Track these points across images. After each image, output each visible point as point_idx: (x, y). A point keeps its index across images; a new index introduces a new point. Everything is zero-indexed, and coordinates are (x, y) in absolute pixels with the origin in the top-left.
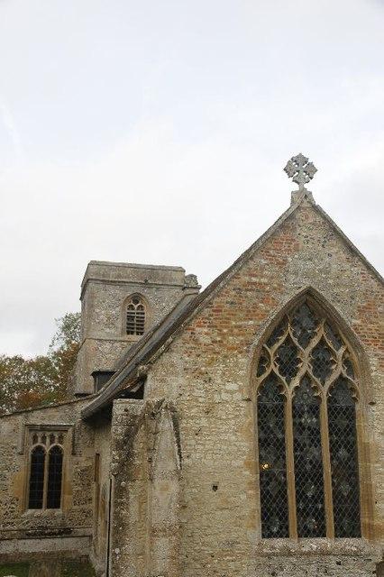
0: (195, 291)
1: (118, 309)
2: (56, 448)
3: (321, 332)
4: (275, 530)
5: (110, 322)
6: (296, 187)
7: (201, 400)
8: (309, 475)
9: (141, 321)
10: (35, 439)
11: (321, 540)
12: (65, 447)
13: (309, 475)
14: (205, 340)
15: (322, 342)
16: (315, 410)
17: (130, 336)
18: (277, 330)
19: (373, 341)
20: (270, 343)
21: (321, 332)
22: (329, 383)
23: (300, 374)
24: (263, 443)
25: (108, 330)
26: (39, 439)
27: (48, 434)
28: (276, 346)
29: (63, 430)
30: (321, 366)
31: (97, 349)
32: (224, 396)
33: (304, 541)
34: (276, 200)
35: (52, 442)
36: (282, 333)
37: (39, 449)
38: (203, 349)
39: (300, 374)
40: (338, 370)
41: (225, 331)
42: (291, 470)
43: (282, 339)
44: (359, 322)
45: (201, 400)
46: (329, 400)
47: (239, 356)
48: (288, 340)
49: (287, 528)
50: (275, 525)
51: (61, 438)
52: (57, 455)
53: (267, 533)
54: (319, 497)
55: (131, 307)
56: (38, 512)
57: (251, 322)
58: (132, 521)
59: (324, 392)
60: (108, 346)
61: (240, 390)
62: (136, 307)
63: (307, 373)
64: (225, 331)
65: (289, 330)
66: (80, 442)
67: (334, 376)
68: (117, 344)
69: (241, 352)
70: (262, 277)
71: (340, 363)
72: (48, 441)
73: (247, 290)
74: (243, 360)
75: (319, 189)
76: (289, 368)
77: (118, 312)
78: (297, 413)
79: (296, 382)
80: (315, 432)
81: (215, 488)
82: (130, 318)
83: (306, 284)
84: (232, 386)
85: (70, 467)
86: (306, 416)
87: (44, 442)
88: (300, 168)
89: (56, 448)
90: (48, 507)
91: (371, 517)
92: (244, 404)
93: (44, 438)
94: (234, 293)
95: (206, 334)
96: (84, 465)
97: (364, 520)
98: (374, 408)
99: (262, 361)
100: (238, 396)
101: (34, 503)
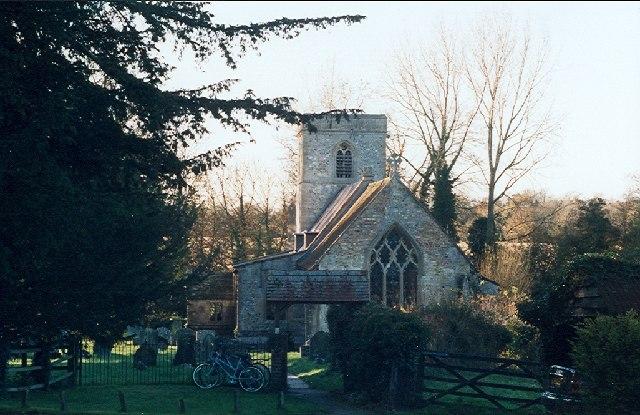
1: (328, 156)
5: (322, 168)
16: (397, 279)
18: (380, 243)
20: (377, 248)
21: (402, 242)
22: (405, 264)
25: (320, 174)
30: (401, 257)
31: (311, 191)
48: (385, 246)
55: (340, 152)
59: (402, 270)
76: (385, 260)
78: (389, 279)
79: (388, 266)
82: (339, 161)
99: (373, 256)
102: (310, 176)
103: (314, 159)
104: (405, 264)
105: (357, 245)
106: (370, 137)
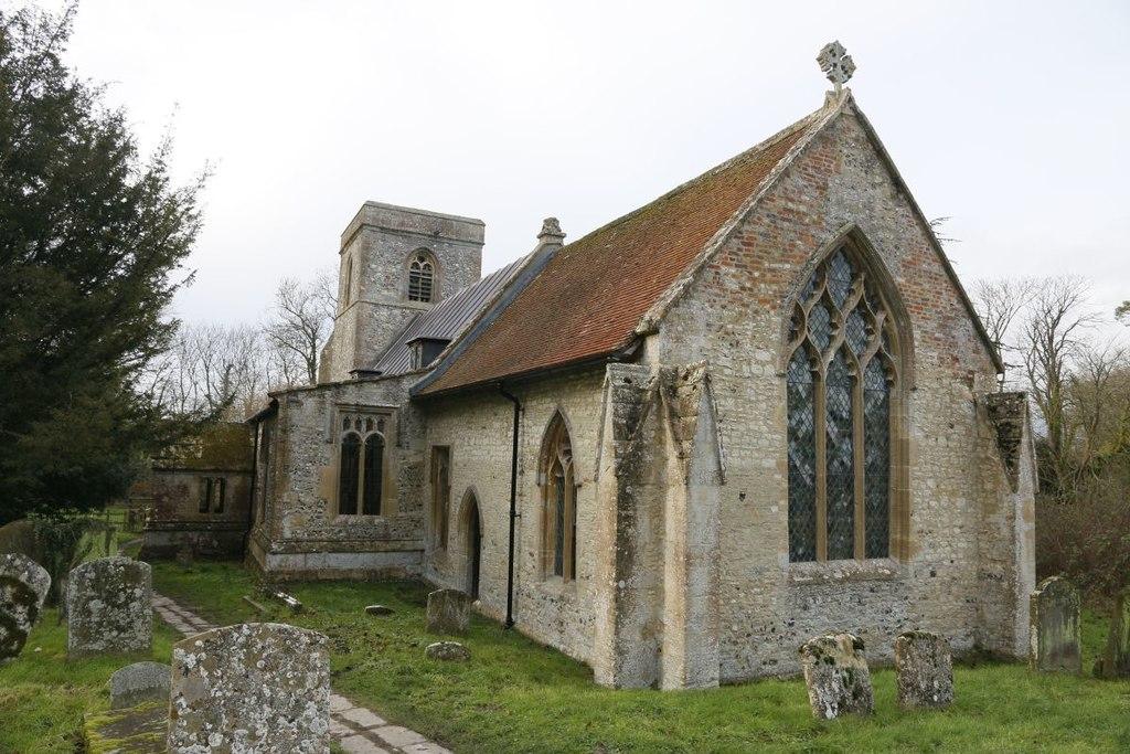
0: (557, 240)
1: (399, 267)
2: (375, 437)
4: (801, 551)
6: (831, 87)
7: (727, 371)
8: (842, 482)
9: (427, 283)
10: (346, 424)
11: (853, 562)
12: (387, 436)
13: (842, 482)
14: (732, 285)
17: (413, 302)
19: (916, 308)
20: (808, 296)
24: (792, 434)
25: (386, 292)
26: (353, 424)
27: (365, 417)
29: (384, 413)
31: (371, 316)
32: (756, 369)
33: (834, 564)
34: (806, 98)
35: (369, 428)
37: (352, 438)
38: (729, 297)
39: (837, 344)
41: (756, 274)
42: (822, 475)
43: (819, 294)
45: (727, 371)
47: (772, 312)
49: (814, 548)
50: (801, 545)
51: (381, 424)
52: (375, 445)
53: (795, 557)
54: (850, 510)
56: (352, 519)
57: (787, 266)
58: (640, 542)
60: (384, 313)
61: (773, 362)
62: (421, 265)
63: (844, 344)
64: (756, 274)
66: (408, 429)
68: (396, 312)
69: (774, 308)
71: (879, 333)
72: (364, 426)
73: (784, 220)
74: (776, 319)
75: (866, 93)
77: (400, 271)
81: (742, 496)
82: (414, 279)
83: (850, 219)
84: (764, 356)
85: (394, 464)
87: (358, 428)
88: (836, 62)
89: (375, 436)
90: (364, 513)
91: (905, 529)
92: (776, 381)
93: (358, 423)
94: (766, 221)
95: (734, 276)
96: (412, 460)
97: (895, 536)
98: (915, 395)
100: (770, 370)
101: (347, 506)
102: (373, 297)
103: (379, 271)
105: (763, 279)
106: (462, 252)
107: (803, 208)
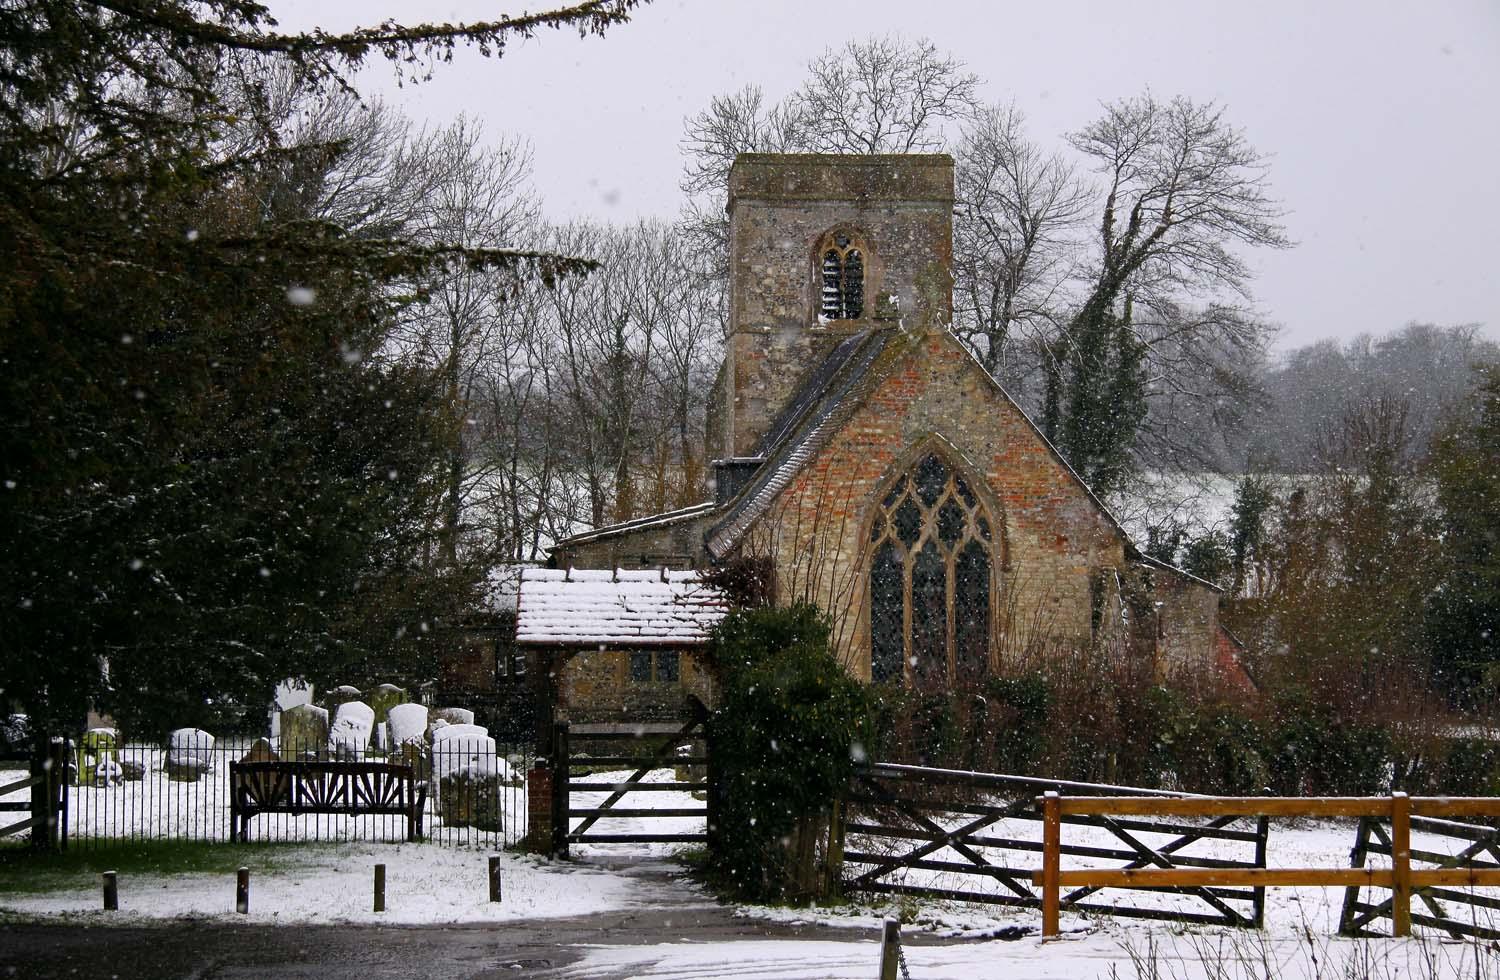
3: (950, 488)
15: (951, 500)
20: (888, 501)
21: (950, 488)
22: (958, 546)
23: (923, 538)
28: (895, 506)
30: (950, 527)
36: (901, 491)
40: (971, 531)
43: (901, 498)
44: (995, 475)
46: (958, 566)
48: (908, 500)
57: (862, 482)
59: (950, 560)
65: (910, 487)
67: (966, 539)
70: (877, 427)
73: (858, 444)
76: (909, 533)
79: (918, 547)
80: (940, 599)
86: (929, 584)
99: (878, 523)
104: (958, 546)
107: (879, 431)
